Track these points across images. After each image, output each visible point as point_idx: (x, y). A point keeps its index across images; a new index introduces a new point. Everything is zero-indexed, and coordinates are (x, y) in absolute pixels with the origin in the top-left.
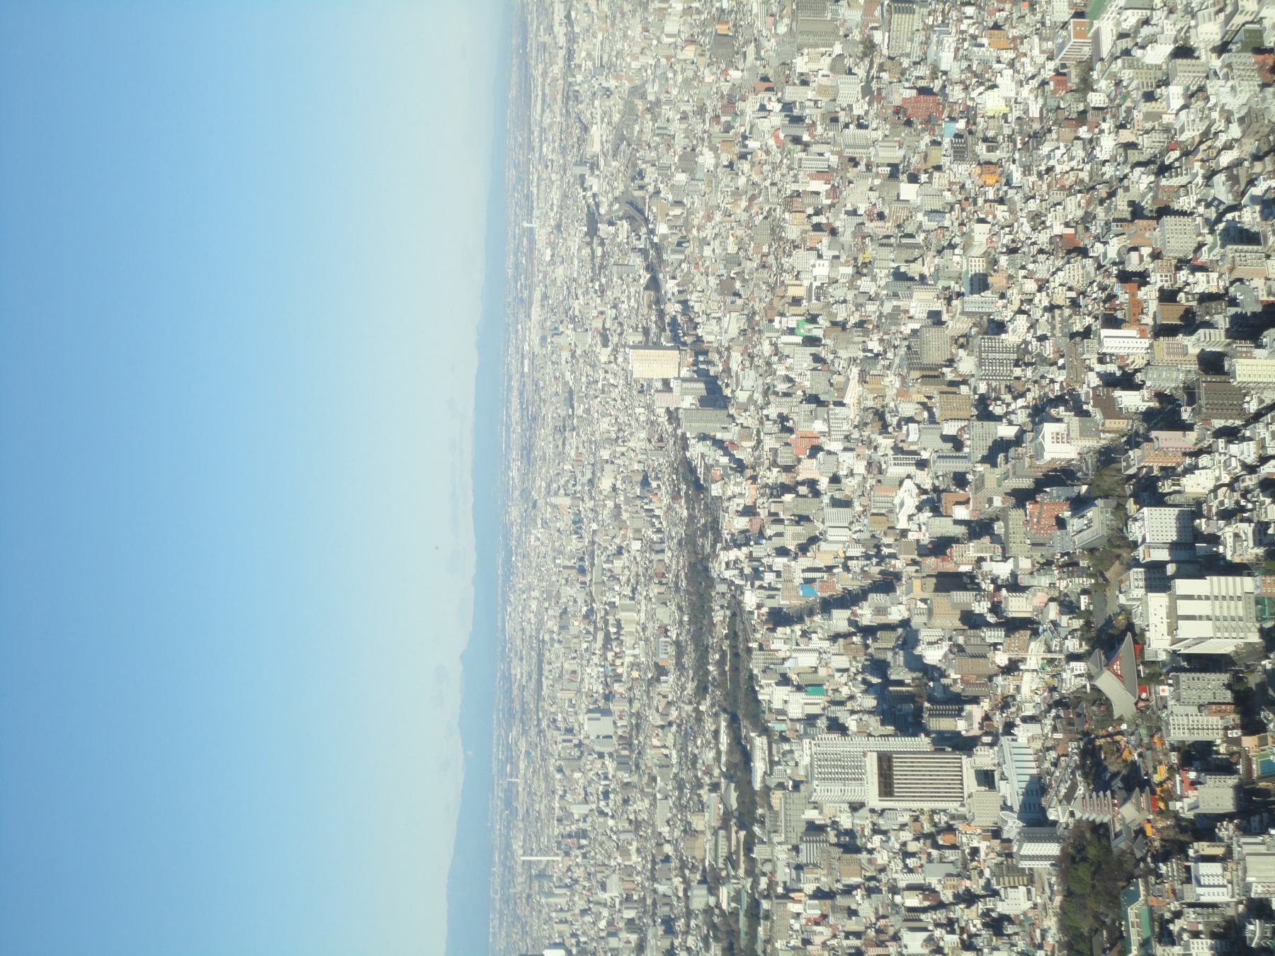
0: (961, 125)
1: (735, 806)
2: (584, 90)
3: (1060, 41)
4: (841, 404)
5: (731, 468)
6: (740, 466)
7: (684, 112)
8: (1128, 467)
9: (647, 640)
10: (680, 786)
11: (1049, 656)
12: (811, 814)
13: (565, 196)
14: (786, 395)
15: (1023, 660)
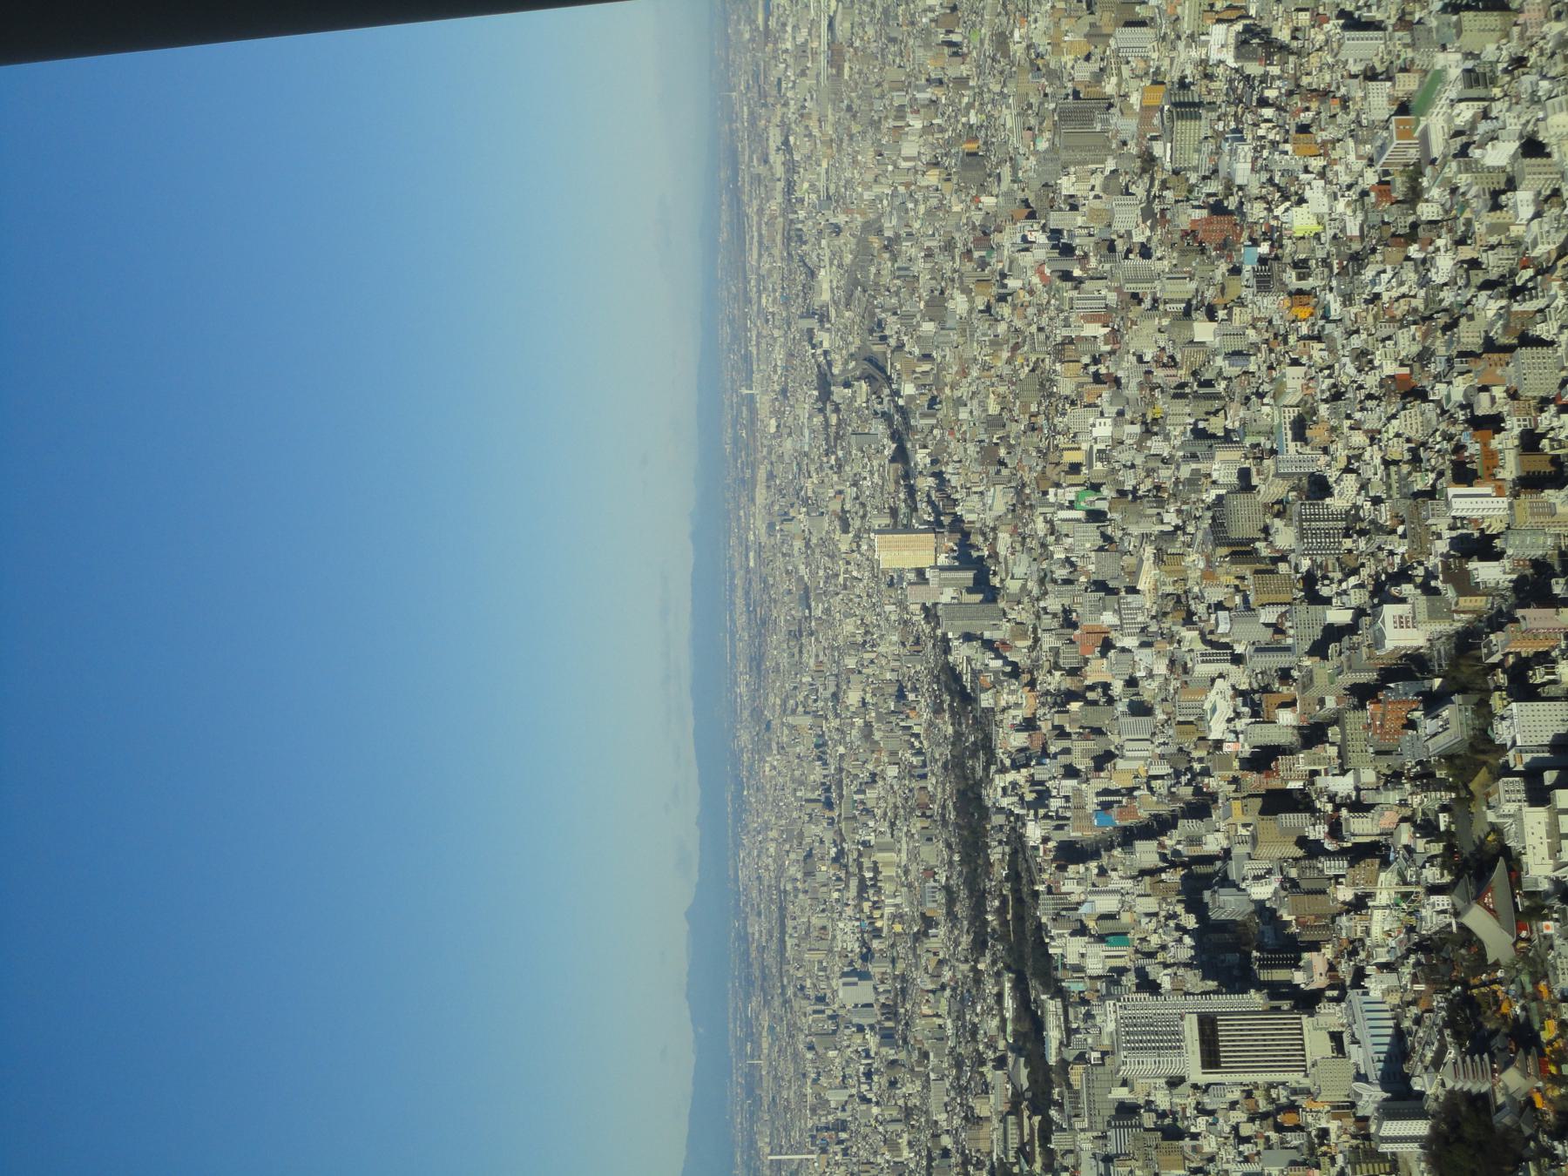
0: (1264, 248)
1: (1026, 1085)
2: (808, 228)
3: (1379, 143)
4: (1132, 590)
5: (1005, 674)
6: (1015, 672)
7: (929, 248)
8: (1491, 654)
9: (910, 886)
10: (959, 1064)
11: (1404, 889)
12: (1121, 1093)
13: (791, 355)
14: (1067, 582)
15: (1371, 895)
